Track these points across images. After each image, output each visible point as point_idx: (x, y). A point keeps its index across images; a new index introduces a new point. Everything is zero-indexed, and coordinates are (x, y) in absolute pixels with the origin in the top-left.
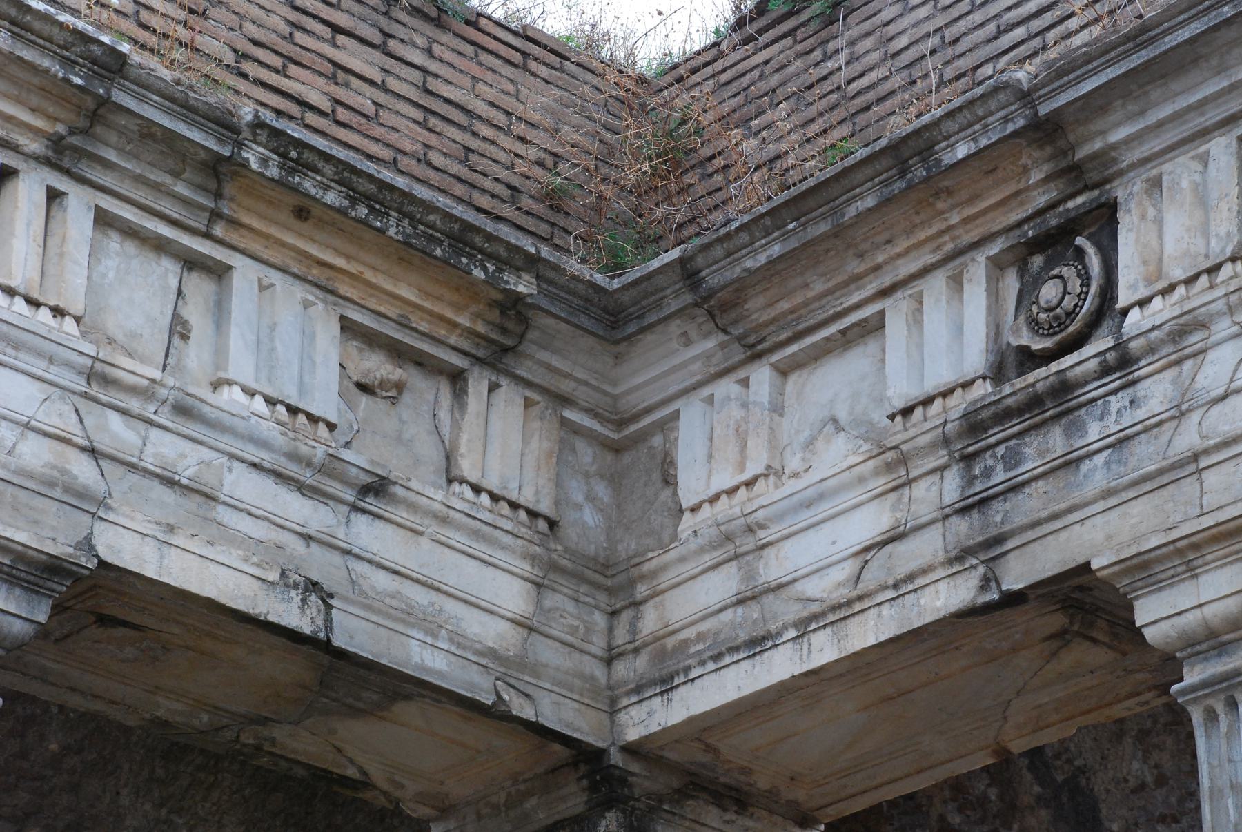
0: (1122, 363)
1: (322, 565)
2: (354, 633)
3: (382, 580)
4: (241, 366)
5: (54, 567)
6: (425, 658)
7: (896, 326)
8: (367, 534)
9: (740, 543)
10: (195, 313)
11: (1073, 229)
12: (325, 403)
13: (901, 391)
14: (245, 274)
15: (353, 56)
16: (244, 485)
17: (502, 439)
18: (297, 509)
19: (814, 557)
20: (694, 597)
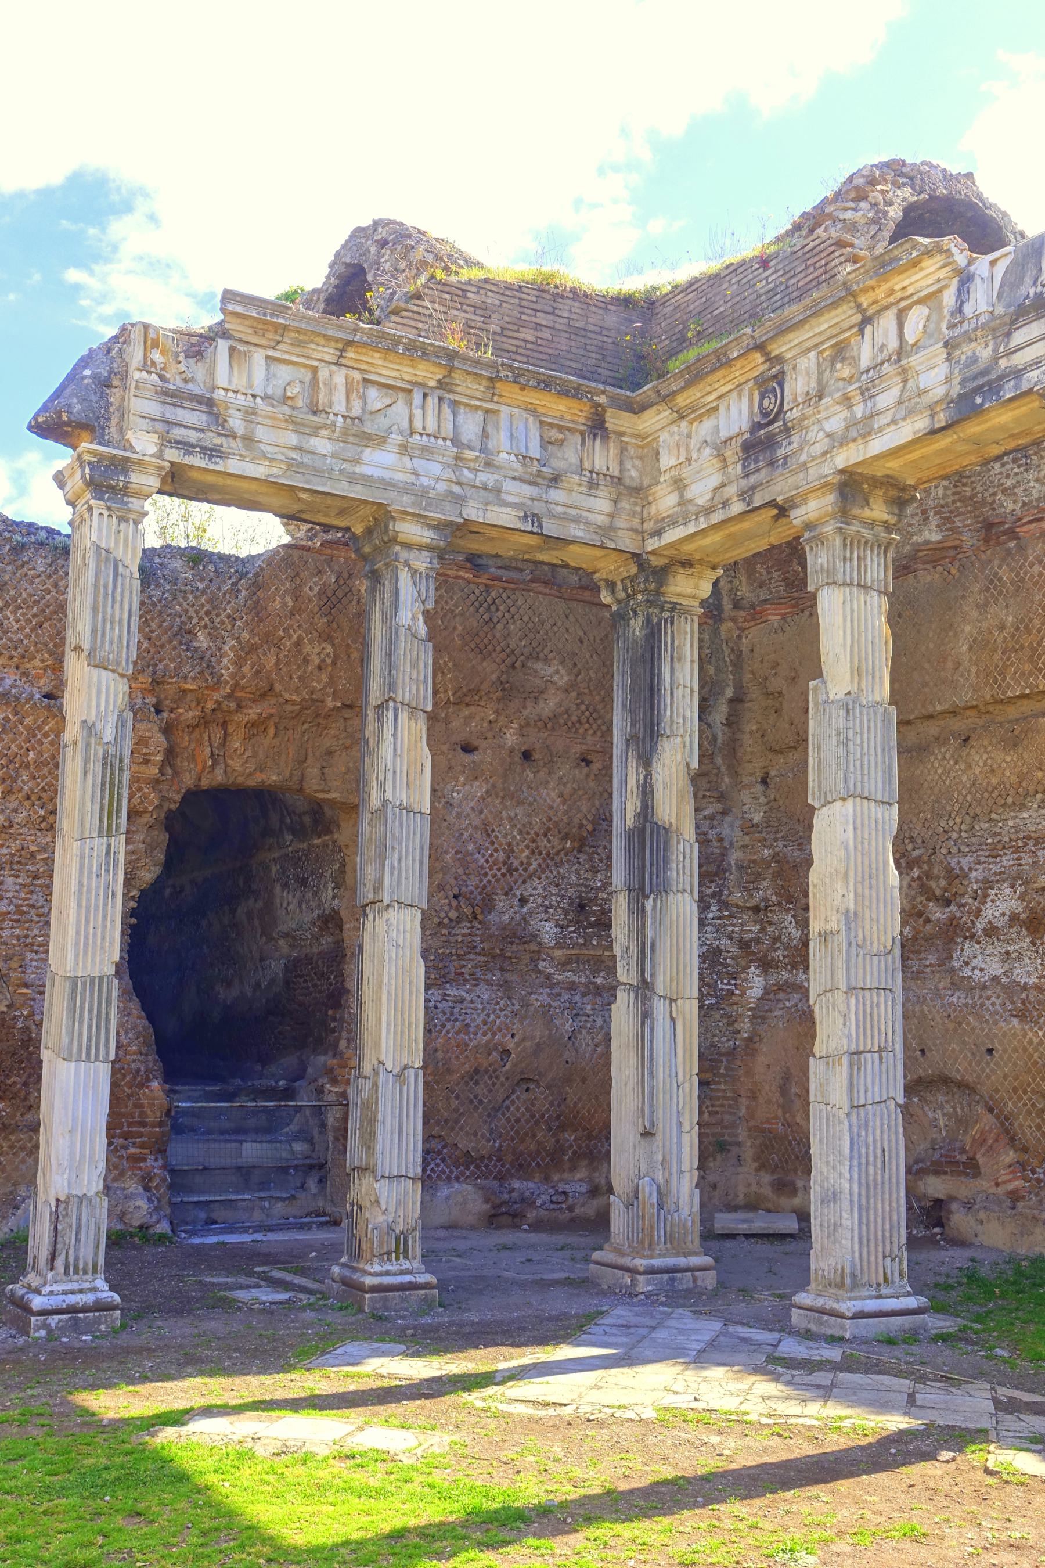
0: (787, 430)
1: (538, 508)
3: (560, 509)
5: (450, 524)
7: (722, 409)
8: (555, 495)
9: (679, 485)
13: (724, 434)
16: (509, 486)
18: (528, 490)
19: (700, 492)
20: (665, 502)
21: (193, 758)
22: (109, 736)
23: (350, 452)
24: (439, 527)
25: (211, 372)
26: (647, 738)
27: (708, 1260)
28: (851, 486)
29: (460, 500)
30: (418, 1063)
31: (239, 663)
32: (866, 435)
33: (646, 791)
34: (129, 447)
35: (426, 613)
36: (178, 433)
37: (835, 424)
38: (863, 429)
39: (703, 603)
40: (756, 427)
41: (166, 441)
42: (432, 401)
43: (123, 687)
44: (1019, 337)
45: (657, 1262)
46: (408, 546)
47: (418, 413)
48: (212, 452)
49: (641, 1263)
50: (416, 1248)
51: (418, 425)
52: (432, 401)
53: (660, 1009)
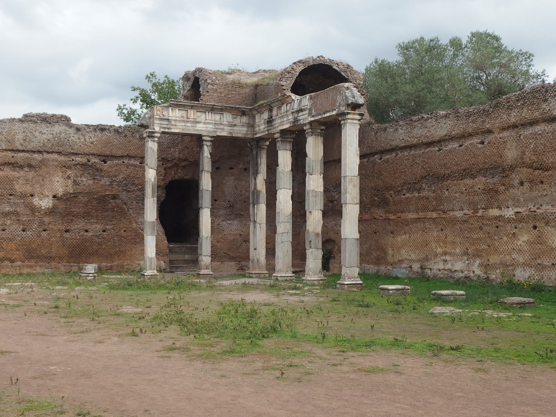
0: (273, 120)
1: (232, 131)
2: (234, 135)
4: (225, 120)
6: (239, 135)
8: (235, 128)
9: (259, 126)
10: (222, 117)
11: (271, 110)
12: (231, 120)
14: (225, 115)
15: (233, 93)
16: (226, 128)
17: (245, 119)
18: (230, 128)
20: (257, 129)
21: (170, 174)
22: (153, 180)
23: (194, 125)
24: (211, 137)
25: (168, 114)
26: (256, 173)
27: (267, 272)
28: (283, 132)
29: (216, 132)
30: (210, 236)
31: (179, 153)
32: (283, 125)
33: (255, 184)
34: (154, 129)
35: (211, 154)
36: (163, 126)
37: (279, 121)
38: (282, 124)
39: (267, 146)
40: (269, 118)
41: (161, 128)
42: (210, 114)
43: (155, 171)
44: (300, 114)
45: (256, 272)
46: (206, 141)
47: (207, 116)
48: (169, 129)
49: (254, 272)
50: (210, 267)
51: (207, 118)
52: (210, 114)
53: (258, 226)
